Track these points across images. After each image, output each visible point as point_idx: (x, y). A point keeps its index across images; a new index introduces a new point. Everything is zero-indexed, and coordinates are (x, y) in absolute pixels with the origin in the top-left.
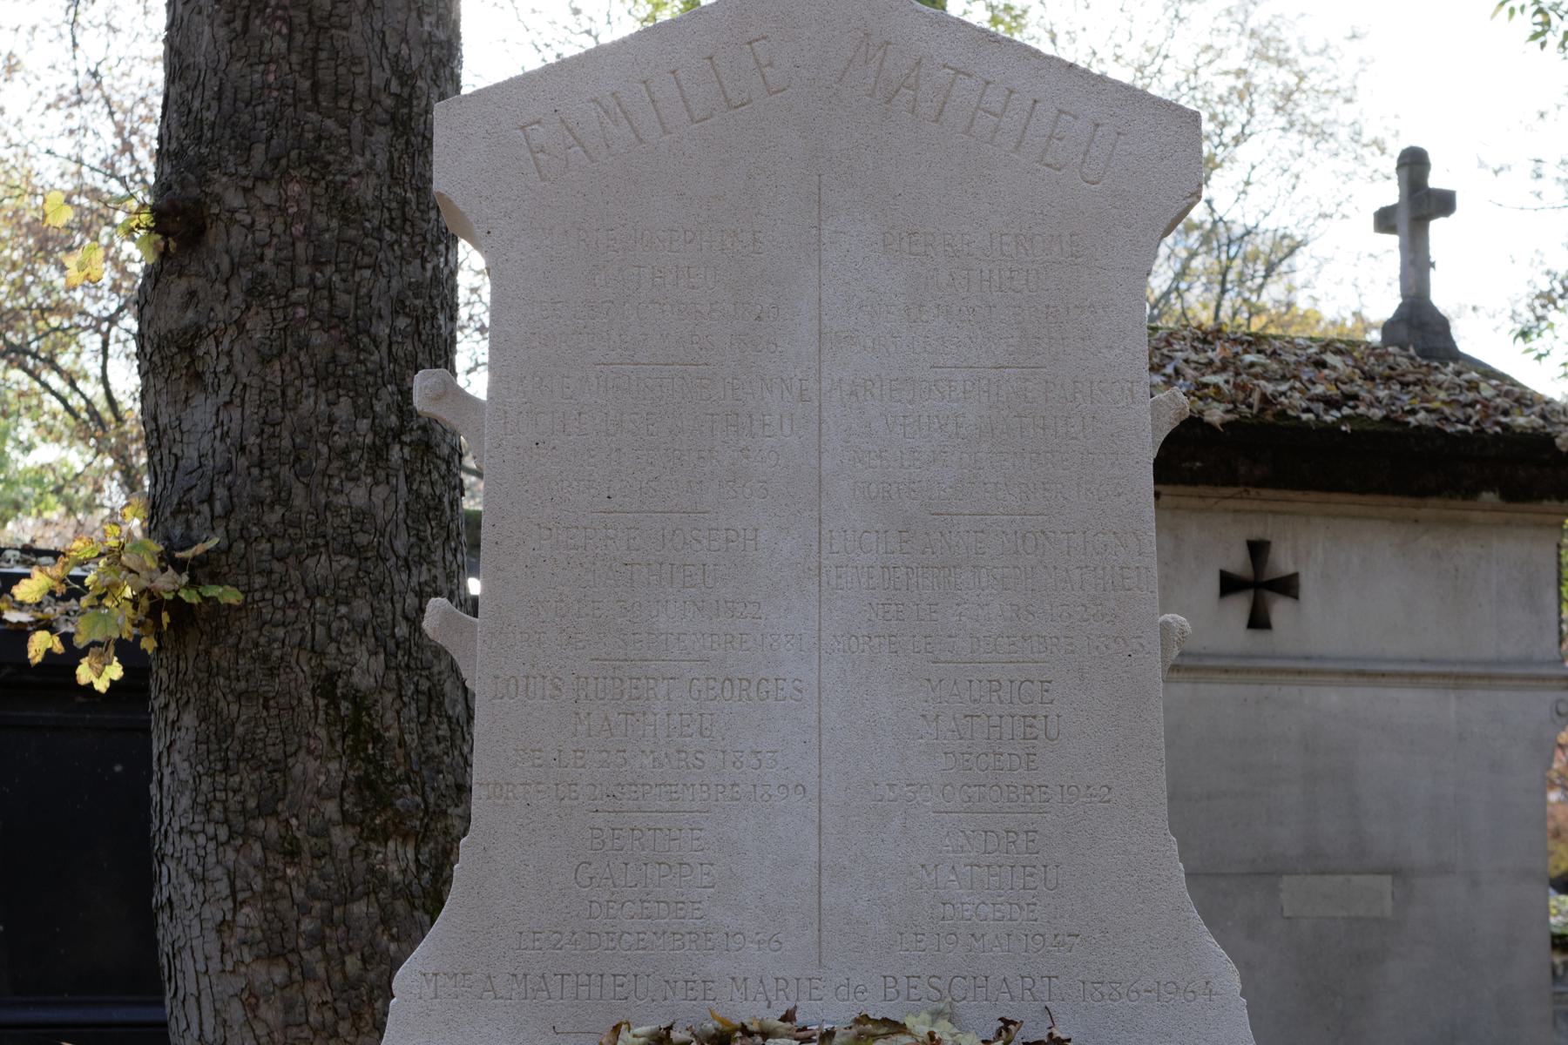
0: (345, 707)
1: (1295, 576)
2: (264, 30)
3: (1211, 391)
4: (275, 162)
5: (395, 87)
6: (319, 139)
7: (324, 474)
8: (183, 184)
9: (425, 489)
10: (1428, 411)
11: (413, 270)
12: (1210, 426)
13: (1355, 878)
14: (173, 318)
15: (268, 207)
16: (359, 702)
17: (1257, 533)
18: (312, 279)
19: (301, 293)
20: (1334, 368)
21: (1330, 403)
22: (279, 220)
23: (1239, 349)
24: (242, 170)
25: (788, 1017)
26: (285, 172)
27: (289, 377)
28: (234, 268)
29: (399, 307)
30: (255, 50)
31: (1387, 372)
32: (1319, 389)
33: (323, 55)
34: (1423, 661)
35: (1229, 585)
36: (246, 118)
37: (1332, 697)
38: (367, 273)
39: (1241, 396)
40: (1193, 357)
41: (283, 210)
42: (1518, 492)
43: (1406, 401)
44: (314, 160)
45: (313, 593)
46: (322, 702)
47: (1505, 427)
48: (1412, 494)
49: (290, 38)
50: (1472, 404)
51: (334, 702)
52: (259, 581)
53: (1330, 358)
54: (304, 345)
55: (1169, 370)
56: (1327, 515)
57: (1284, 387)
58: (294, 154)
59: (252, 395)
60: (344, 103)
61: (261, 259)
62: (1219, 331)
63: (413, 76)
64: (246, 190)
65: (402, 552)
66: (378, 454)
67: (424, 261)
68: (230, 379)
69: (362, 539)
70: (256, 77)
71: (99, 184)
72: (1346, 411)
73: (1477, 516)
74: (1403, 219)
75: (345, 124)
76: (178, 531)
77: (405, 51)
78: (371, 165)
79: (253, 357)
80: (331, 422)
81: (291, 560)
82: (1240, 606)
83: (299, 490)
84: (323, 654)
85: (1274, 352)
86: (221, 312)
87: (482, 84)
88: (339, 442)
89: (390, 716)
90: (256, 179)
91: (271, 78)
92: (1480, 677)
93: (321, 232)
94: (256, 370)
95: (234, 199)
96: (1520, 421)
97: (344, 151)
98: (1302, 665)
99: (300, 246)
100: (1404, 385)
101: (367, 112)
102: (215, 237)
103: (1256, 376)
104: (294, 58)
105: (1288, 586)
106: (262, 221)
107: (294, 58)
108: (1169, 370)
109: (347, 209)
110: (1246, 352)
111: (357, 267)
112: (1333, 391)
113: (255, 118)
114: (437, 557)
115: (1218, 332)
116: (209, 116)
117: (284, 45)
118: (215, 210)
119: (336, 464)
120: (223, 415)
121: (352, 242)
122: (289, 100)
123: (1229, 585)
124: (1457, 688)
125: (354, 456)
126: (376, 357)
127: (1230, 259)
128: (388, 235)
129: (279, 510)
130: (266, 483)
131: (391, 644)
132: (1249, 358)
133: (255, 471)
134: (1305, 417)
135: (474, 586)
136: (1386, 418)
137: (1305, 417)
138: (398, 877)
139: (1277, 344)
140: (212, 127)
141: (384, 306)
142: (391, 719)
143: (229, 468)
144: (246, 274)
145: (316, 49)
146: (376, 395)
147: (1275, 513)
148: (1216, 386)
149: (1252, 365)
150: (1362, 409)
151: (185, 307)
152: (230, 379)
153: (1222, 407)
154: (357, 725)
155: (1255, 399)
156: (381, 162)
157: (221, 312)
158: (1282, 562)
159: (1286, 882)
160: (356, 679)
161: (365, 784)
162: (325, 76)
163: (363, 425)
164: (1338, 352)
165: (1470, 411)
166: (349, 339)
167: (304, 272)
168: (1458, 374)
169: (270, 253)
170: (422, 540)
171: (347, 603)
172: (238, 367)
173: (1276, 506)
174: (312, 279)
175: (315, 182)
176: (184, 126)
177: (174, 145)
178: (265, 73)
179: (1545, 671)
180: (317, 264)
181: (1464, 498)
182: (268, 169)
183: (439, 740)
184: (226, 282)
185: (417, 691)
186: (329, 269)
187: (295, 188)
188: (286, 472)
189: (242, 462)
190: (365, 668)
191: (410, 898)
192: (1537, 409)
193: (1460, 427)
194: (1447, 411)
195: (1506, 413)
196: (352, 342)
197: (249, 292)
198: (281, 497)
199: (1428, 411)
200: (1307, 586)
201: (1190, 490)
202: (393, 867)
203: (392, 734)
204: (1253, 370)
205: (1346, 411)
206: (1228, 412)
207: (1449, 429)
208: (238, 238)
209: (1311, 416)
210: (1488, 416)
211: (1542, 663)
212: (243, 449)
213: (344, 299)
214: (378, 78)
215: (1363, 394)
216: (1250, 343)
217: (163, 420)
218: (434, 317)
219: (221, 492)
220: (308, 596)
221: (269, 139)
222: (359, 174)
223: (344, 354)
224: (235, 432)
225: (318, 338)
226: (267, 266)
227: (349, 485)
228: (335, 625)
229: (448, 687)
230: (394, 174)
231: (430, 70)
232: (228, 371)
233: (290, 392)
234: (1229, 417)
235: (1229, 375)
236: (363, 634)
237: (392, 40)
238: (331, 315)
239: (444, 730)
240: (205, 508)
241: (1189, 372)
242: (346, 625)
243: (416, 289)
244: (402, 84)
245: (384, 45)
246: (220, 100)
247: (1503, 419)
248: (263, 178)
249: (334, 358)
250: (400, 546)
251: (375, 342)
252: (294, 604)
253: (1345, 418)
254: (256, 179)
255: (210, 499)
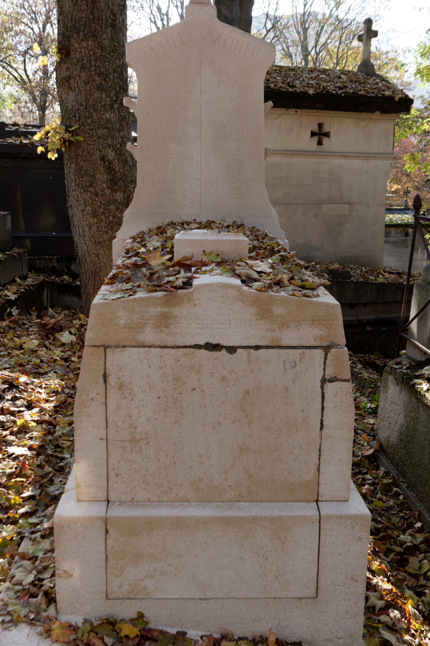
0: (107, 163)
1: (329, 132)
2: (81, 3)
3: (310, 85)
4: (85, 36)
5: (112, 17)
6: (95, 31)
7: (100, 111)
8: (65, 42)
9: (122, 114)
10: (364, 90)
11: (117, 62)
12: (309, 95)
13: (340, 205)
14: (65, 74)
15: (84, 48)
16: (110, 162)
17: (320, 121)
18: (95, 65)
19: (93, 68)
20: (343, 79)
21: (340, 88)
22: (87, 51)
23: (320, 74)
24: (78, 38)
25: (195, 220)
26: (88, 39)
27: (91, 88)
28: (77, 62)
29: (115, 71)
30: (79, 8)
31: (356, 80)
32: (338, 85)
33: (95, 9)
34: (359, 153)
35: (313, 134)
36: (78, 25)
37: (337, 162)
38: (107, 63)
39: (318, 86)
40: (308, 76)
41: (88, 48)
42: (384, 111)
43: (360, 87)
44: (94, 36)
45: (99, 138)
46: (102, 162)
47: (383, 95)
48: (358, 112)
49: (87, 5)
50: (375, 89)
51: (104, 162)
52: (87, 135)
53: (343, 76)
54: (94, 80)
55: (301, 79)
56: (338, 117)
57: (329, 84)
58: (89, 34)
59: (83, 93)
60: (100, 21)
61: (83, 60)
62: (315, 68)
63: (116, 14)
64: (79, 43)
65: (118, 128)
66: (112, 106)
67: (120, 60)
68: (78, 89)
69: (109, 126)
70: (80, 15)
71: (19, 10)
72: (344, 90)
73: (375, 117)
74: (364, 38)
75: (101, 27)
76: (68, 124)
77: (114, 8)
78: (107, 37)
79: (83, 83)
80: (101, 98)
81: (94, 130)
82: (315, 139)
83: (95, 115)
84: (102, 151)
85: (329, 74)
86: (75, 73)
87: (135, 37)
88: (103, 103)
89: (117, 165)
90: (81, 40)
91: (83, 15)
92: (373, 157)
93: (97, 53)
94: (84, 86)
95: (76, 45)
96: (387, 93)
97: (101, 33)
98: (330, 154)
99: (92, 57)
100: (360, 83)
101: (105, 24)
102: (72, 54)
103: (323, 81)
104: (88, 10)
105: (327, 135)
106: (83, 50)
107: (88, 10)
108: (301, 79)
109: (102, 47)
110: (321, 74)
111: (105, 62)
112: (341, 85)
113: (80, 26)
114: (125, 129)
115: (315, 69)
116: (69, 25)
117: (86, 7)
118: (72, 48)
119: (103, 108)
120: (77, 97)
121: (104, 56)
122: (88, 21)
123: (313, 134)
124: (367, 160)
125: (106, 106)
126: (110, 83)
127: (343, 34)
128: (112, 54)
129: (90, 119)
130: (87, 113)
131: (116, 149)
132: (322, 76)
133: (85, 110)
134: (333, 92)
135: (134, 134)
136: (353, 92)
137: (333, 92)
138: (119, 200)
139: (330, 72)
140: (70, 27)
141: (111, 71)
142: (117, 166)
143: (79, 109)
144: (80, 63)
145: (93, 8)
146: (111, 92)
147: (325, 116)
148: (312, 84)
149: (322, 78)
150: (348, 90)
151: (66, 71)
152: (78, 89)
153: (313, 89)
154: (110, 167)
155: (321, 87)
156: (110, 36)
157: (75, 73)
158: (326, 129)
159: (324, 205)
160: (109, 157)
161: (112, 180)
162: (96, 15)
163: (108, 99)
164: (345, 74)
165: (374, 90)
166: (104, 79)
167: (93, 63)
168: (374, 80)
169: (85, 58)
170: (122, 126)
171: (106, 140)
172: (79, 86)
173: (326, 114)
174: (95, 65)
175: (95, 41)
176: (64, 27)
177: (62, 32)
178: (82, 14)
179: (388, 156)
180: (96, 61)
181: (372, 113)
182: (84, 38)
183: (127, 170)
184: (76, 66)
185: (122, 160)
186: (99, 62)
187: (90, 43)
188: (91, 110)
189: (82, 108)
190: (111, 154)
191: (122, 204)
192: (392, 90)
193: (372, 95)
194: (369, 90)
195: (384, 91)
196: (105, 80)
197: (81, 68)
198: (91, 116)
199: (364, 90)
200: (332, 135)
201: (304, 110)
202: (118, 198)
203: (117, 169)
204: (322, 79)
205: (344, 90)
206: (314, 91)
207: (369, 95)
208: (78, 55)
209: (335, 92)
210: (379, 92)
211: (388, 154)
212: (82, 105)
213: (102, 69)
214: (108, 15)
215: (349, 86)
216: (323, 72)
217: (63, 98)
218: (123, 73)
219: (77, 115)
220: (98, 138)
221: (84, 31)
222: (104, 39)
223: (103, 83)
224: (80, 101)
225: (97, 79)
226: (85, 62)
227: (106, 113)
228: (104, 145)
229: (129, 159)
230: (113, 39)
231: (120, 13)
232: (77, 87)
233: (92, 92)
234: (314, 92)
235: (316, 81)
236: (110, 147)
237: (111, 5)
238: (100, 73)
239: (128, 168)
240: (74, 118)
241: (306, 80)
242: (106, 145)
243: (118, 66)
244: (113, 16)
245: (109, 6)
246: (72, 21)
247: (383, 93)
248: (82, 40)
249: (101, 84)
250: (117, 127)
251: (110, 80)
252: (95, 141)
253: (343, 92)
254: (81, 40)
255: (75, 116)
